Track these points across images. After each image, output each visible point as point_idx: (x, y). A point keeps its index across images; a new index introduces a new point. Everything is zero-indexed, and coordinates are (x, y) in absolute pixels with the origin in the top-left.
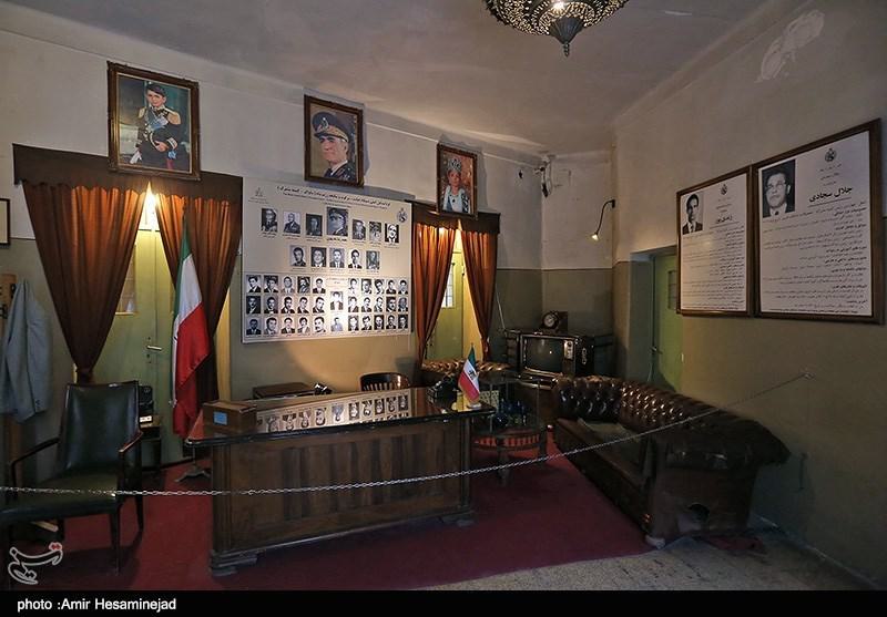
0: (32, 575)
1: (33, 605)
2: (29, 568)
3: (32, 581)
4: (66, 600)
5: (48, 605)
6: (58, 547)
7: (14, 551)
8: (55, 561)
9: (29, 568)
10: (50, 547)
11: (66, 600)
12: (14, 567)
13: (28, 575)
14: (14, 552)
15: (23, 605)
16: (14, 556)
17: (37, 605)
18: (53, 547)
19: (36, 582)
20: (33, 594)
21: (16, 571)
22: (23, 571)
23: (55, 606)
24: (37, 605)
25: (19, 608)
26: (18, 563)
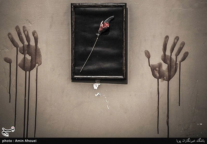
0: (7, 134)
2: (7, 133)
3: (8, 136)
4: (16, 140)
5: (11, 141)
6: (14, 128)
7: (3, 129)
8: (13, 131)
9: (7, 133)
11: (16, 140)
12: (3, 132)
13: (6, 134)
14: (3, 129)
16: (3, 130)
18: (12, 128)
19: (9, 136)
22: (5, 133)
25: (3, 142)
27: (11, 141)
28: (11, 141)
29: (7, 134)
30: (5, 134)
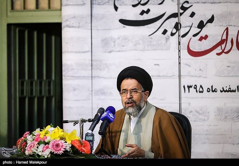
0: (8, 155)
1: (7, 163)
5: (11, 163)
6: (15, 147)
10: (13, 147)
12: (3, 153)
13: (7, 155)
15: (4, 163)
17: (8, 163)
18: (14, 147)
20: (7, 160)
21: (4, 154)
22: (6, 153)
23: (13, 163)
24: (8, 163)
25: (3, 163)
26: (6, 152)
27: (10, 162)
28: (10, 162)
29: (8, 154)
30: (7, 156)
